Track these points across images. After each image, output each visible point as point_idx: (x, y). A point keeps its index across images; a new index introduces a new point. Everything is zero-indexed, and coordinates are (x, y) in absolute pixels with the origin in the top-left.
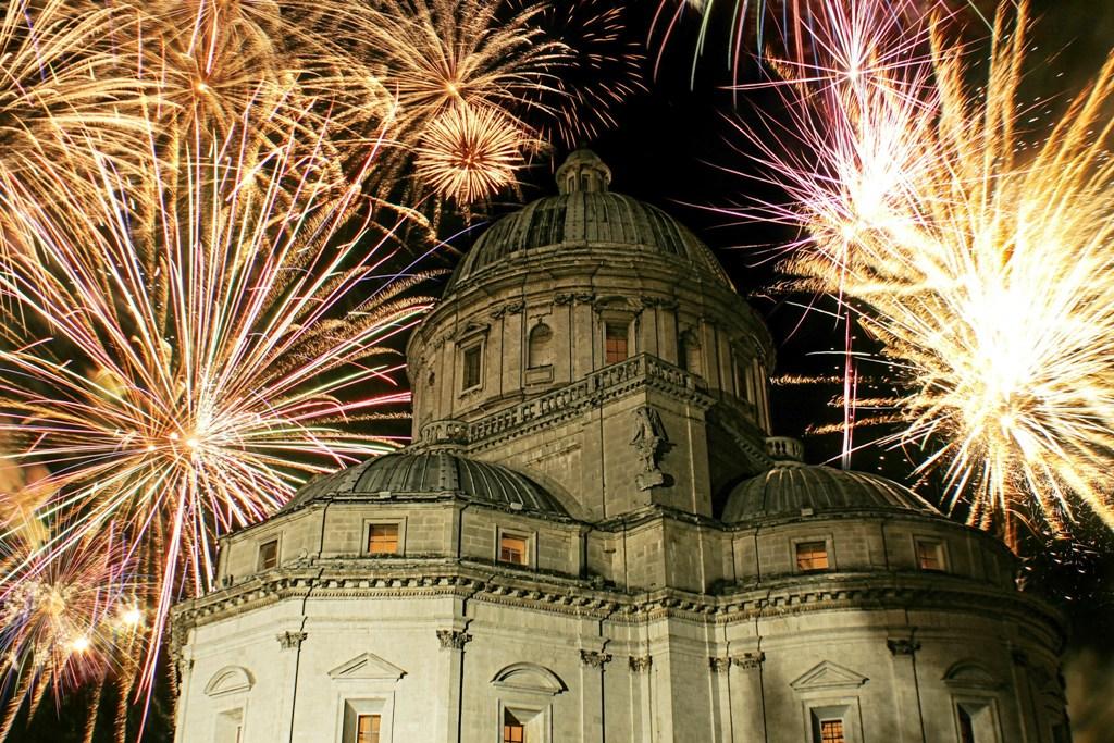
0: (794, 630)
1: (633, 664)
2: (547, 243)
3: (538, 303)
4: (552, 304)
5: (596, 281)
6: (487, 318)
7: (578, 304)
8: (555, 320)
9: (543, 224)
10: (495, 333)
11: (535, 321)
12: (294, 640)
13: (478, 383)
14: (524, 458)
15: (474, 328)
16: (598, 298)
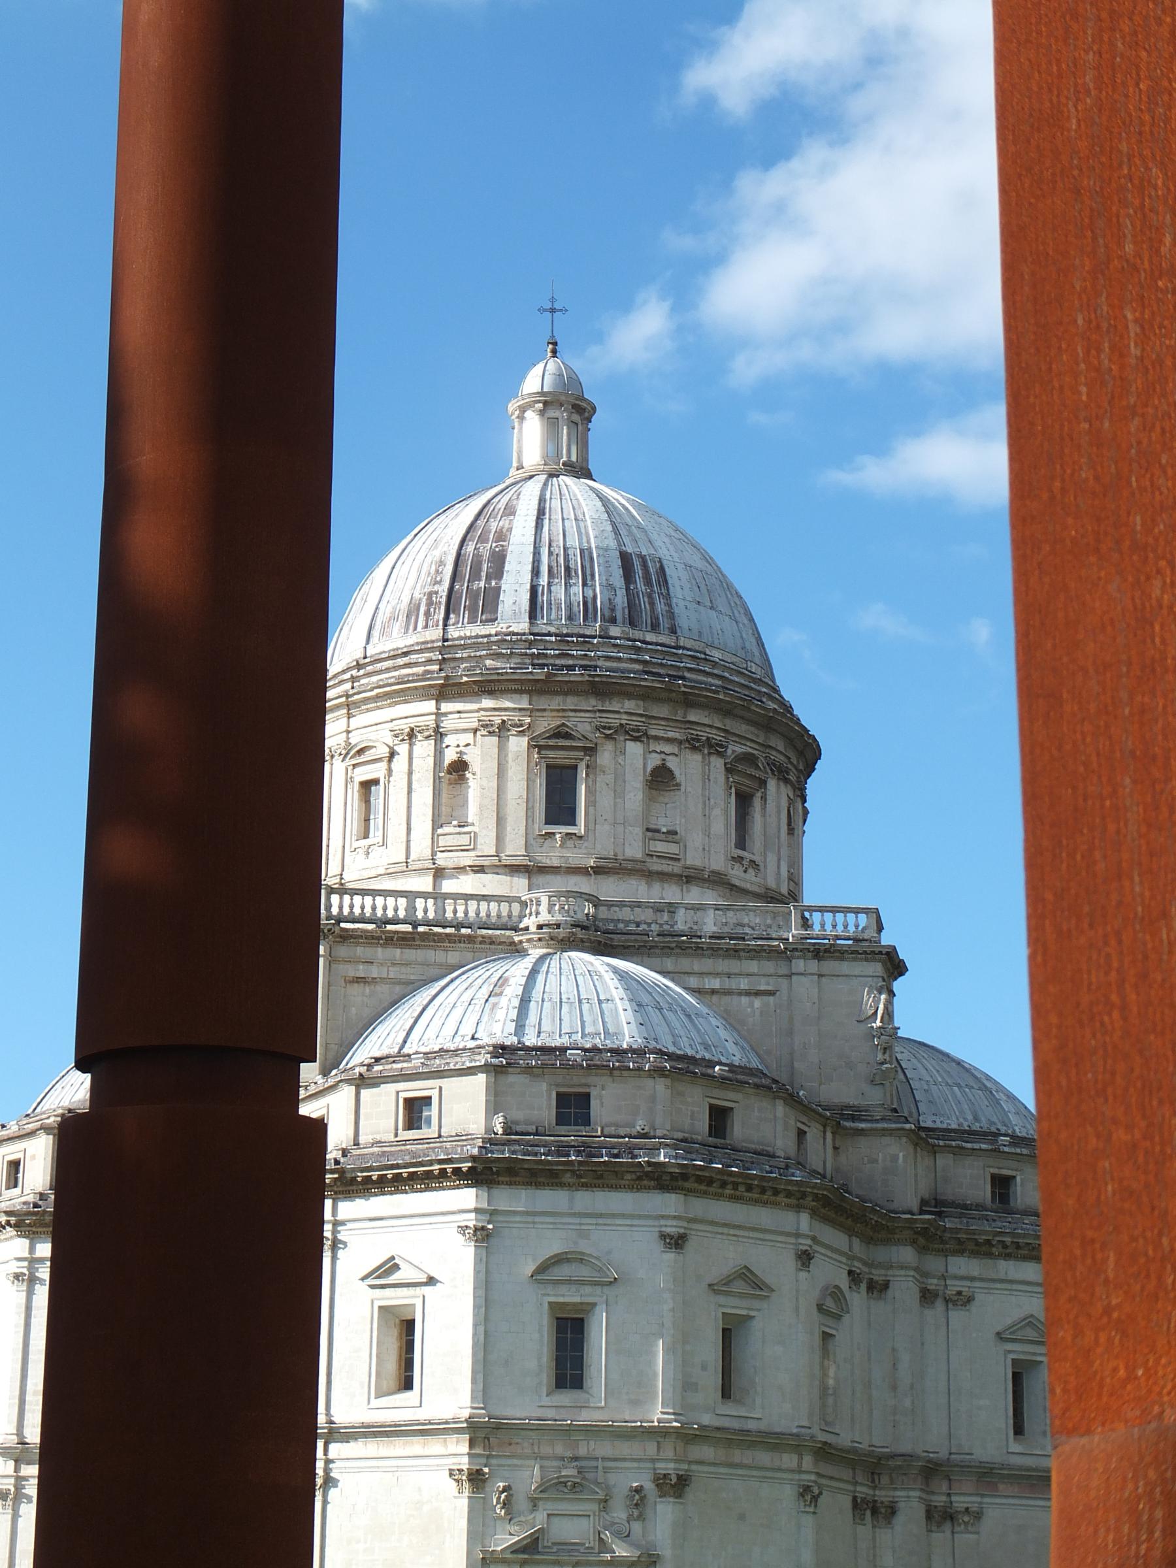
0: (1002, 1276)
1: (872, 1287)
2: (655, 627)
3: (661, 734)
4: (680, 742)
5: (730, 724)
6: (588, 727)
7: (710, 754)
9: (640, 585)
10: (605, 757)
11: (654, 761)
12: (676, 1242)
13: (574, 824)
14: (693, 982)
15: (568, 736)
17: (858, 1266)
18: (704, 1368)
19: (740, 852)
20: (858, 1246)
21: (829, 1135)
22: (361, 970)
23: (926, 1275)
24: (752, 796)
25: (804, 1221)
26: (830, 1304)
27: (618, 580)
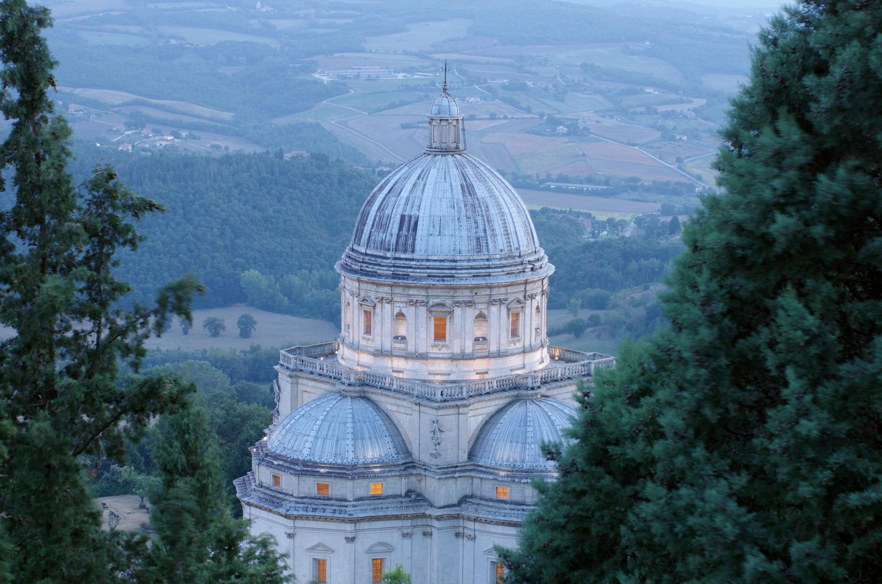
1: (425, 534)
2: (405, 251)
3: (398, 300)
5: (430, 292)
8: (409, 311)
9: (404, 232)
10: (378, 310)
11: (396, 311)
12: (290, 536)
14: (389, 407)
16: (431, 303)
17: (405, 531)
18: (304, 576)
19: (437, 343)
20: (408, 523)
21: (403, 480)
22: (305, 388)
23: (459, 527)
24: (445, 320)
25: (349, 527)
26: (381, 548)
27: (395, 231)
